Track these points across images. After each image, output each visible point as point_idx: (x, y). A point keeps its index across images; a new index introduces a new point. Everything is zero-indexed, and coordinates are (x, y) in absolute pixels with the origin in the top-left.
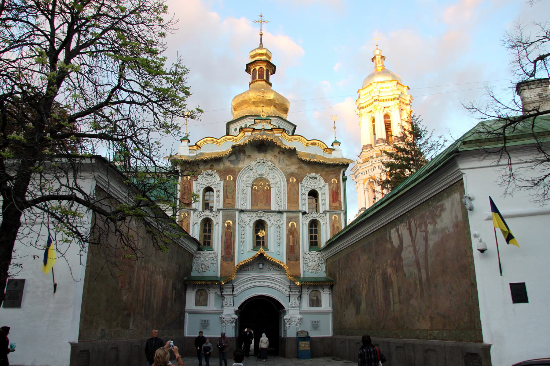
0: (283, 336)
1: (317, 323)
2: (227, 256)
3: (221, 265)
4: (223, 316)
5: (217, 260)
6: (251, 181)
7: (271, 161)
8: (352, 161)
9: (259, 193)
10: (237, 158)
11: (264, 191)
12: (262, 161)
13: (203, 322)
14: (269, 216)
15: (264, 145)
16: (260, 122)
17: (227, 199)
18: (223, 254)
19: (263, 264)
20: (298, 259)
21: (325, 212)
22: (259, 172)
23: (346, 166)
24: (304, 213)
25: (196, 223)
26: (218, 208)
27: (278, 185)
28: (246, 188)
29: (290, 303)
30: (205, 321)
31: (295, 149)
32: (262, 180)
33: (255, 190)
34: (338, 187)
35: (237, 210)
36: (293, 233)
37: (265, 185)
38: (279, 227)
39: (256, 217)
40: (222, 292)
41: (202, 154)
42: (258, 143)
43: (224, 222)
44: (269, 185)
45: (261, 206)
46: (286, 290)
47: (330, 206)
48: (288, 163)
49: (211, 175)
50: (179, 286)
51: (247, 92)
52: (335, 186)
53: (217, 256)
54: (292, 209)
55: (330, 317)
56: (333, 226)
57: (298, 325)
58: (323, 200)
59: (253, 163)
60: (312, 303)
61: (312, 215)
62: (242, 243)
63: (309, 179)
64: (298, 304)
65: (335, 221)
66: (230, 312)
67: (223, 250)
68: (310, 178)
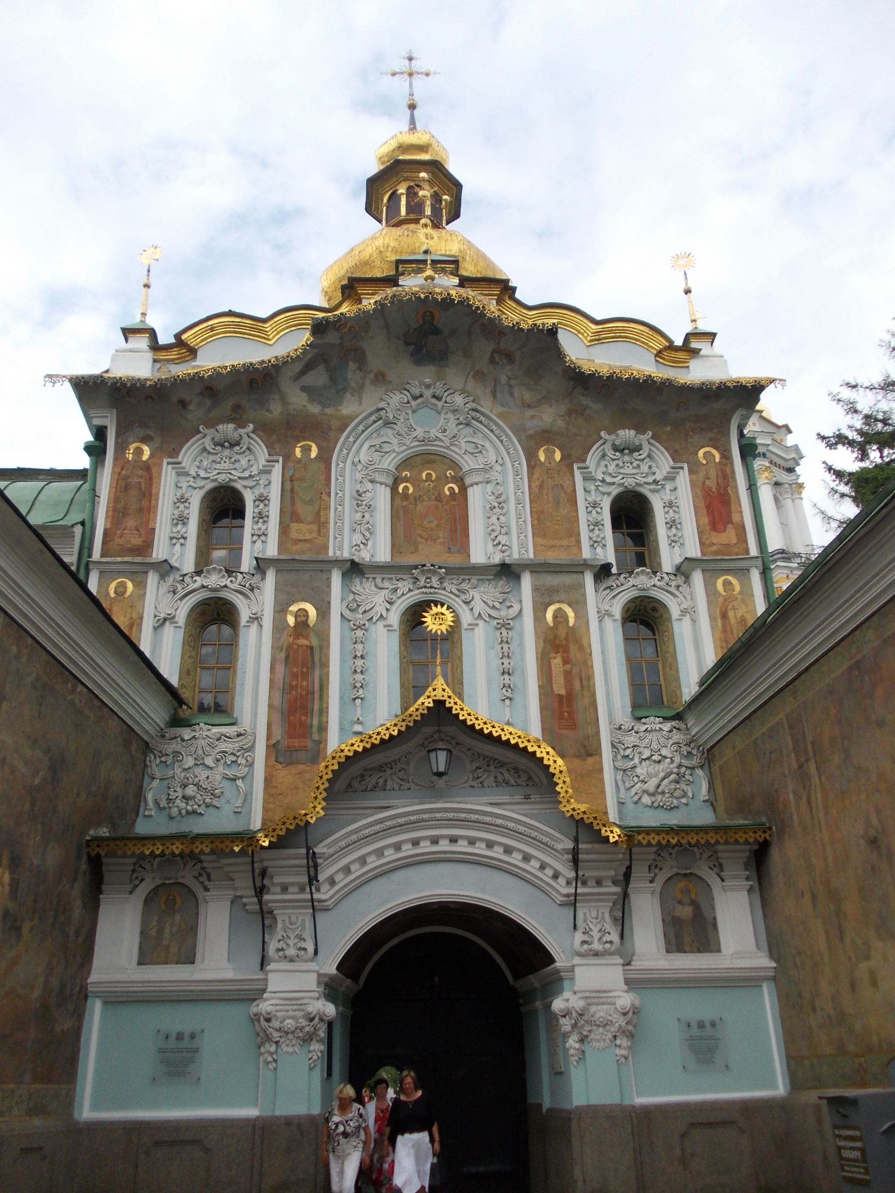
0: (547, 1104)
1: (709, 1030)
2: (296, 743)
3: (268, 780)
4: (265, 1006)
5: (251, 765)
6: (389, 463)
7: (463, 391)
8: (772, 381)
9: (419, 507)
10: (332, 379)
11: (439, 499)
12: (428, 393)
13: (172, 1043)
14: (464, 586)
15: (436, 332)
16: (420, 271)
17: (294, 526)
18: (278, 735)
19: (449, 751)
20: (588, 750)
21: (683, 571)
22: (419, 432)
23: (747, 394)
24: (603, 572)
25: (169, 619)
26: (260, 556)
27: (494, 475)
28: (369, 486)
29: (579, 937)
30: (180, 1037)
31: (553, 332)
32: (431, 462)
33: (405, 496)
34: (725, 476)
35: (337, 562)
36: (562, 647)
37: (443, 479)
38: (504, 626)
39: (408, 597)
40: (260, 891)
41: (194, 367)
42: (414, 325)
43: (281, 610)
44: (460, 480)
45: (431, 553)
46: (556, 876)
47: (701, 543)
48: (527, 396)
49: (232, 445)
50: (48, 856)
51: (374, 238)
52: (713, 473)
53: (251, 749)
54: (552, 557)
55: (768, 998)
56: (724, 616)
57: (623, 1041)
58: (672, 524)
59: (396, 399)
60: (678, 936)
61: (632, 581)
62: (356, 692)
63: (610, 453)
64: (615, 937)
65: (728, 599)
66: (300, 985)
67: (277, 718)
68: (616, 448)
